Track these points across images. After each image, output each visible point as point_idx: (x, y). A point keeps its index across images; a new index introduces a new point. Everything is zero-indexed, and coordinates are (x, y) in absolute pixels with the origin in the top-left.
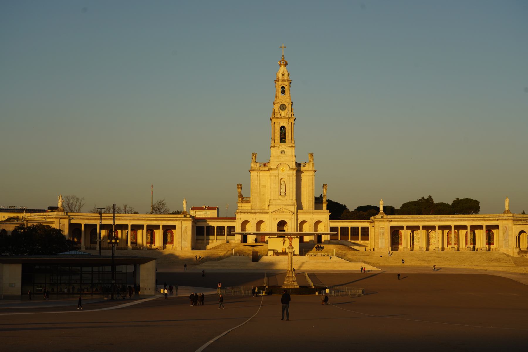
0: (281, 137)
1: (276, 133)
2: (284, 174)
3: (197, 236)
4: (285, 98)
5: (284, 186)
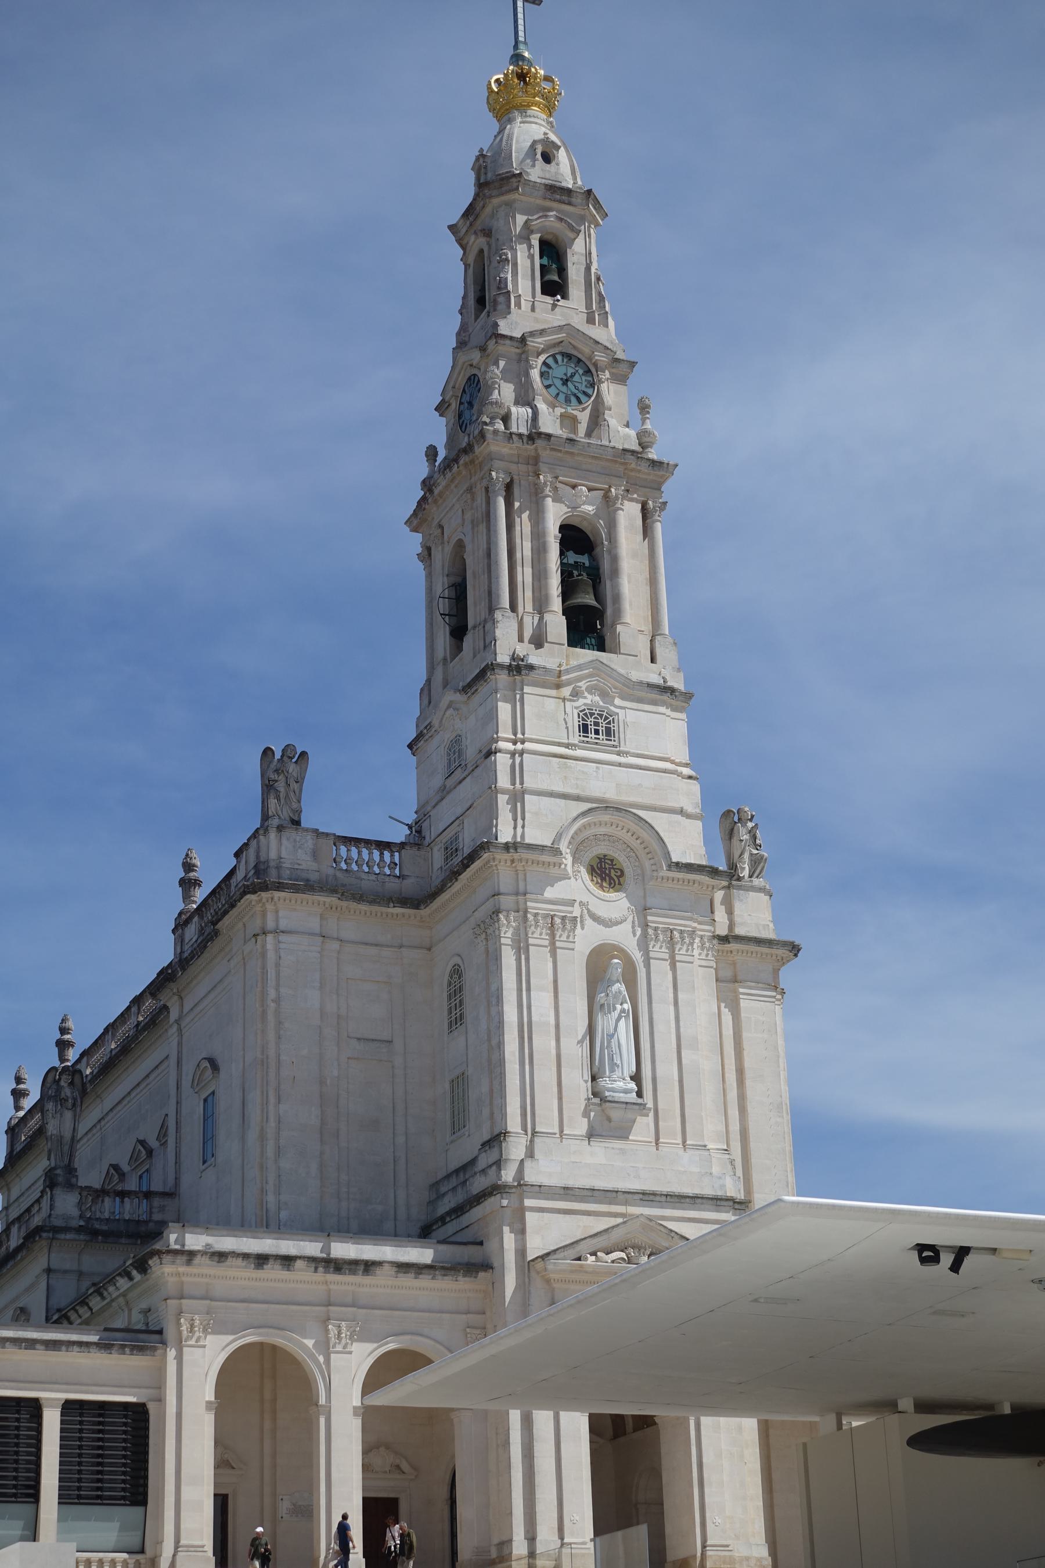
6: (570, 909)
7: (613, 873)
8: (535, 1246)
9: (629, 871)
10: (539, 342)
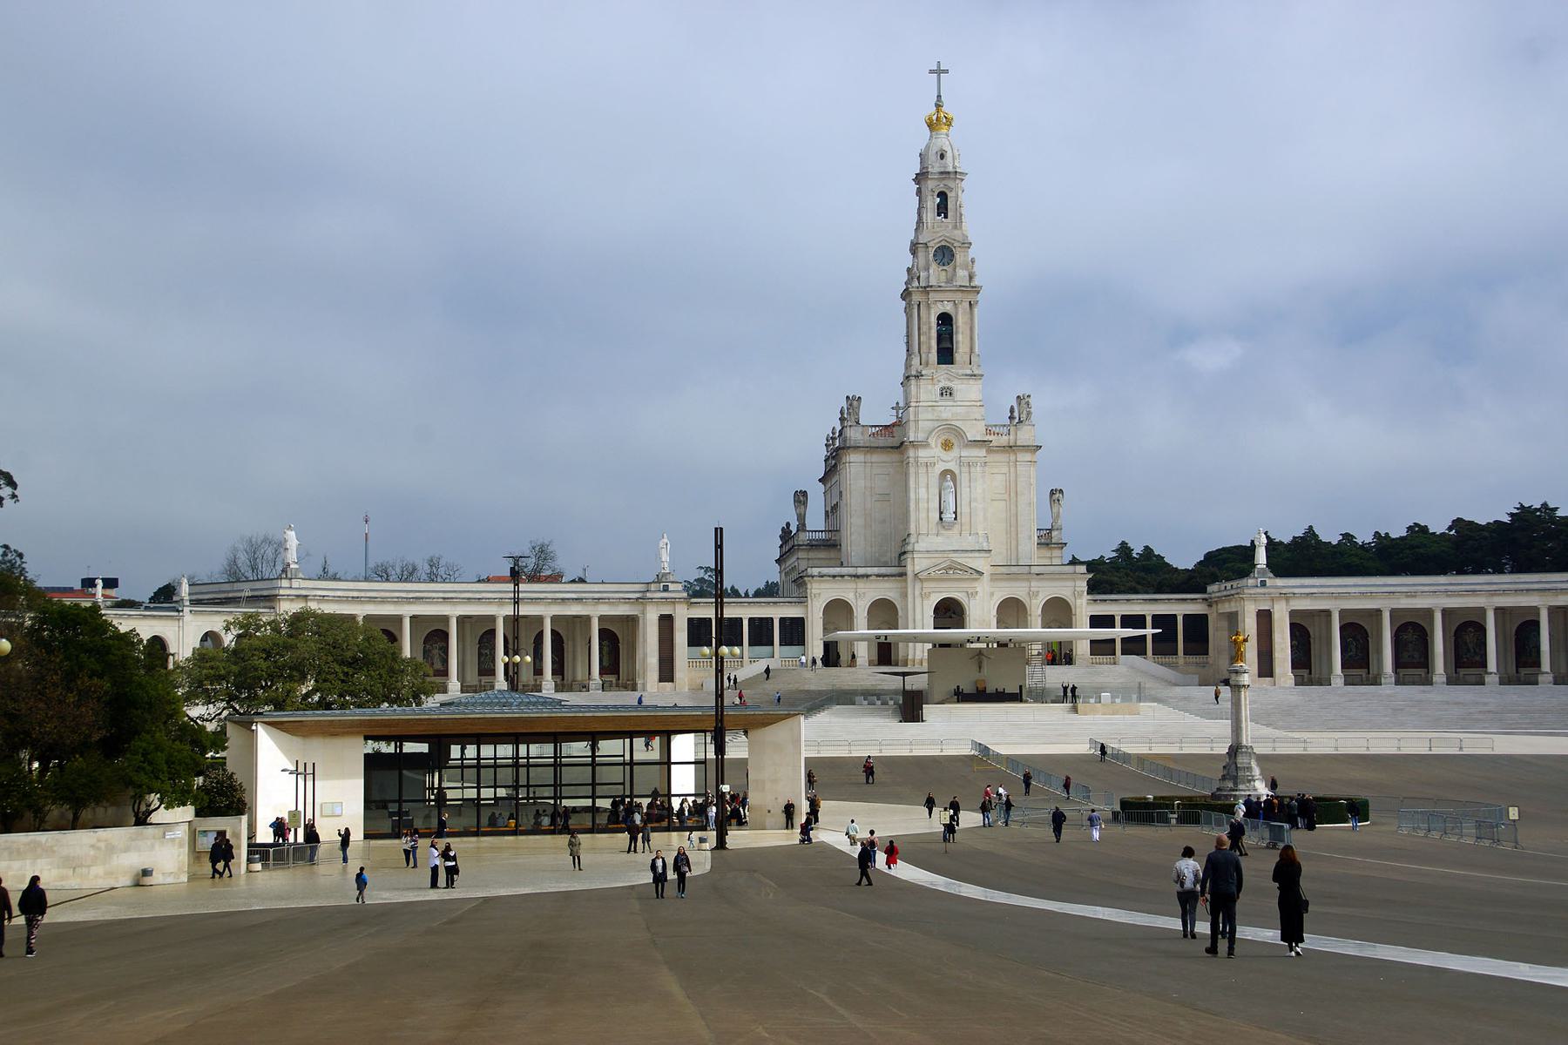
0: (940, 346)
2: (950, 459)
3: (751, 648)
8: (917, 569)
9: (955, 444)
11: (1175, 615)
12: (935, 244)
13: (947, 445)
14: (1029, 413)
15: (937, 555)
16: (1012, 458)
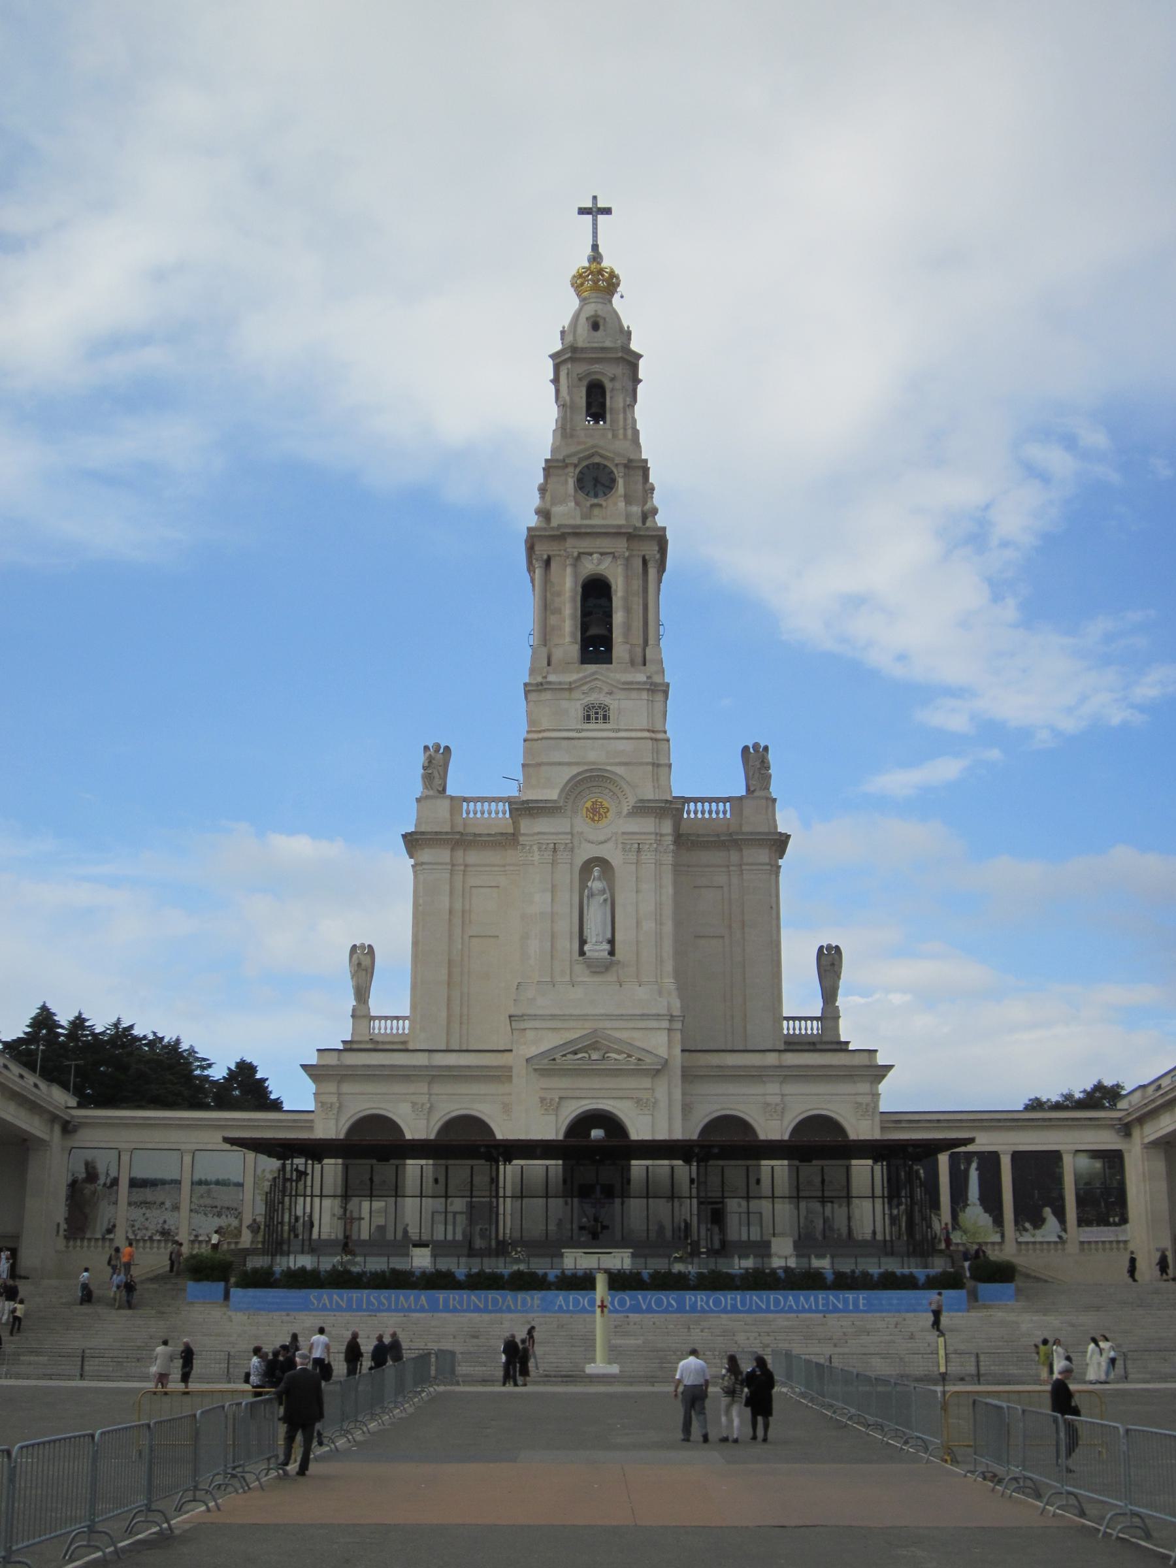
1: (558, 611)
2: (602, 838)
4: (610, 436)
5: (605, 900)
6: (569, 837)
7: (601, 810)
8: (533, 1051)
10: (575, 460)
11: (1058, 1152)
12: (581, 460)
13: (596, 813)
14: (765, 779)
15: (572, 1024)
16: (734, 857)
